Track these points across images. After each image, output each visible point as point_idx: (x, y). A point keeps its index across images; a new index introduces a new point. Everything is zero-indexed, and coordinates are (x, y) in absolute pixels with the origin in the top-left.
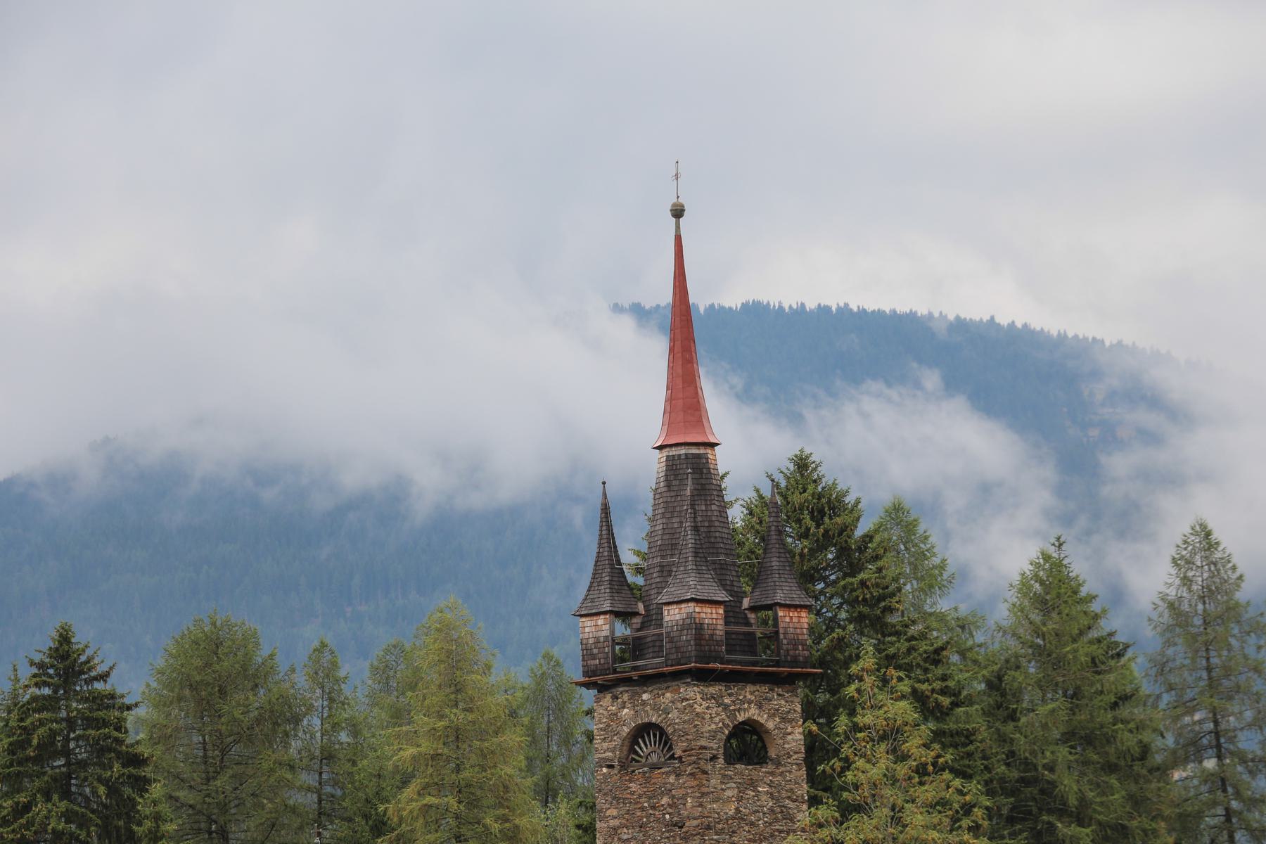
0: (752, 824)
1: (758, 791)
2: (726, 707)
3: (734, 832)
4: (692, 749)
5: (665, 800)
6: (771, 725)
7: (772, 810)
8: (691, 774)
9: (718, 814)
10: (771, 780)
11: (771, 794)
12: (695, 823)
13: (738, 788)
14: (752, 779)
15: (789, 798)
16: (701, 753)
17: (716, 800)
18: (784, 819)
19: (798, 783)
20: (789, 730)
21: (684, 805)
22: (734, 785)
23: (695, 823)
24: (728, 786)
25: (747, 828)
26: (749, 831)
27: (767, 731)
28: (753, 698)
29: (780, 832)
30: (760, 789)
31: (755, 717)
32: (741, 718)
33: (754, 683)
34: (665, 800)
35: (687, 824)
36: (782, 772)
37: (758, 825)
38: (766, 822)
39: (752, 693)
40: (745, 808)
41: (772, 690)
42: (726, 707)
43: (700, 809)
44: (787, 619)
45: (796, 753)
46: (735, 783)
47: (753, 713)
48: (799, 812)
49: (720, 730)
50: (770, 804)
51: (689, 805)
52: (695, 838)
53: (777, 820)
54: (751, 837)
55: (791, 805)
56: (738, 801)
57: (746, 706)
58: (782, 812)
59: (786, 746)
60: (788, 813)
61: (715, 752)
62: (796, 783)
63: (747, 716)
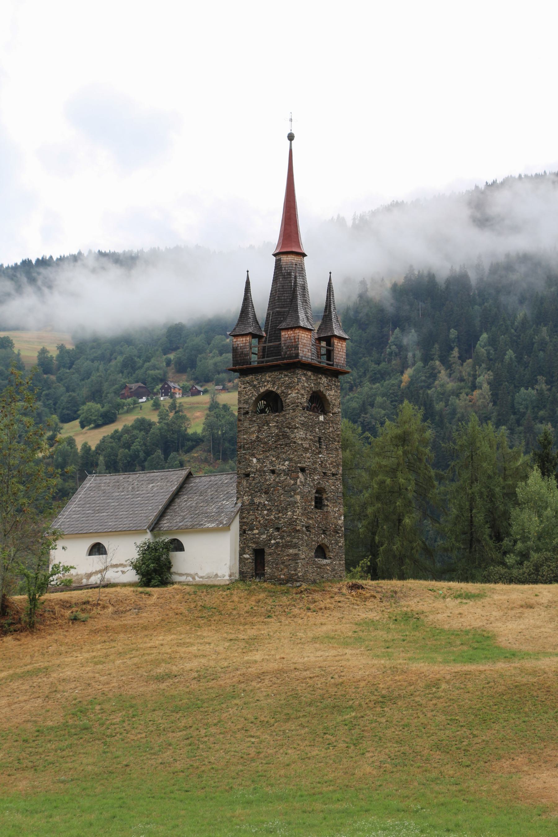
0: (266, 443)
2: (254, 386)
3: (255, 448)
7: (277, 435)
11: (277, 426)
15: (287, 427)
17: (246, 433)
20: (290, 392)
25: (262, 445)
28: (270, 379)
29: (281, 445)
31: (270, 389)
32: (262, 390)
33: (271, 372)
39: (270, 377)
41: (282, 373)
42: (254, 386)
44: (287, 336)
45: (293, 404)
47: (269, 387)
49: (250, 398)
53: (280, 439)
55: (288, 430)
56: (258, 432)
57: (266, 384)
60: (286, 435)
62: (292, 419)
63: (266, 388)
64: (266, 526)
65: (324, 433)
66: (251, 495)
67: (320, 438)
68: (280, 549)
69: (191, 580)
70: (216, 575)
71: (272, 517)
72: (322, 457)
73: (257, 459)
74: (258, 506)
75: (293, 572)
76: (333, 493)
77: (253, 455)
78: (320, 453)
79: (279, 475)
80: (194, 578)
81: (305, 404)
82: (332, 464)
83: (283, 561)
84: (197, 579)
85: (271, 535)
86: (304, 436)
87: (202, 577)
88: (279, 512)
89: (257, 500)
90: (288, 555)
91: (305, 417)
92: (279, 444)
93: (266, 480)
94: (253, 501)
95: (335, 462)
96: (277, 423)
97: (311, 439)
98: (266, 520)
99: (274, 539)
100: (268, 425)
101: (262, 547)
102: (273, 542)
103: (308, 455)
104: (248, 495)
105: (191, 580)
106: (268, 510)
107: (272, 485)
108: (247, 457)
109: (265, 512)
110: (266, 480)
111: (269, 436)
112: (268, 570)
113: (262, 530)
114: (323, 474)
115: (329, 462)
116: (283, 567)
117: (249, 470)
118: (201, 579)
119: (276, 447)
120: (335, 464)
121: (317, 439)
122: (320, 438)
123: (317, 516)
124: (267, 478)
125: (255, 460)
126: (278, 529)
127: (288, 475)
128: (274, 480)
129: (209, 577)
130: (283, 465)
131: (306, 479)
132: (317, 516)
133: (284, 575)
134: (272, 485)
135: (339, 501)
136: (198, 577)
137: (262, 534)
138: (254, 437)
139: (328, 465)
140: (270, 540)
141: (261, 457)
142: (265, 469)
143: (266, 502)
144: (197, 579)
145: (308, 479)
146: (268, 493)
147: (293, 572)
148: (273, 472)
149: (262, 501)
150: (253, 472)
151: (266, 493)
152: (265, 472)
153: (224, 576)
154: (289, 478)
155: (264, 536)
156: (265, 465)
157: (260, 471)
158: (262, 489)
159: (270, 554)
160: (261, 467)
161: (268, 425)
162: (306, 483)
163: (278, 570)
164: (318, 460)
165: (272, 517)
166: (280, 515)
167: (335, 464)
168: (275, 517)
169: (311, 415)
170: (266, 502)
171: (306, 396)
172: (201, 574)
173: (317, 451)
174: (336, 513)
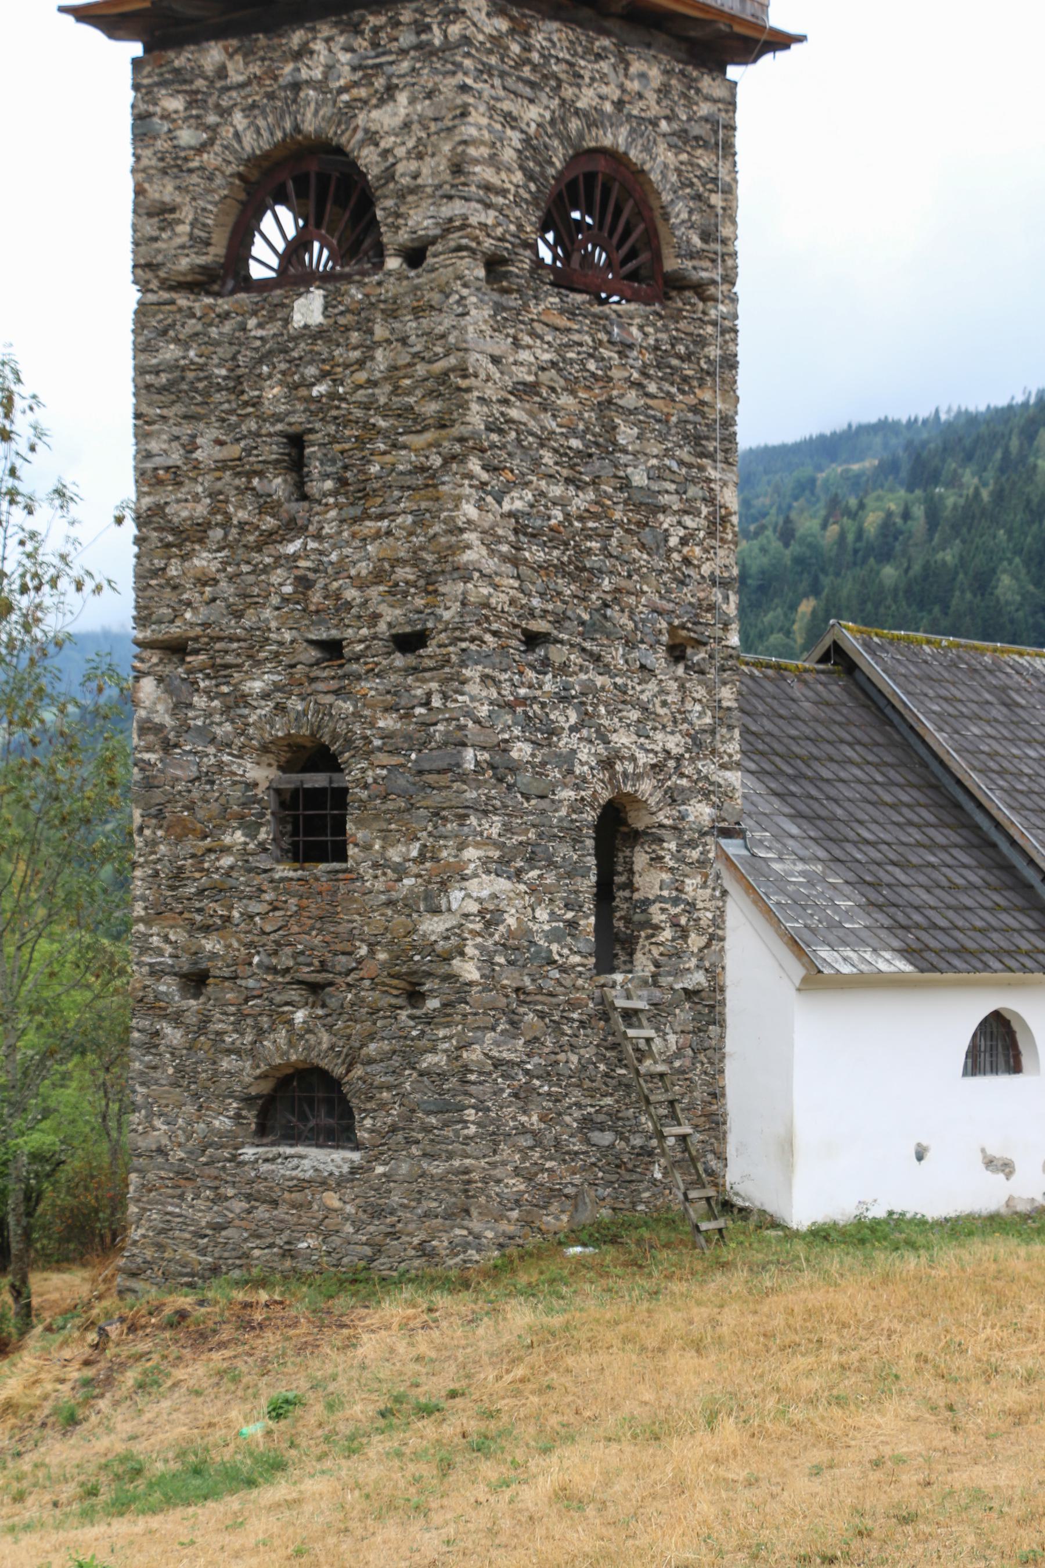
65: (332, 396)
67: (296, 442)
72: (304, 553)
76: (383, 758)
78: (292, 528)
81: (184, 263)
82: (378, 576)
86: (176, 458)
91: (184, 344)
95: (415, 560)
97: (223, 465)
103: (204, 561)
114: (314, 654)
115: (364, 568)
120: (405, 573)
121: (271, 451)
122: (296, 442)
123: (255, 907)
131: (180, 706)
132: (255, 907)
135: (436, 798)
139: (351, 594)
145: (200, 701)
162: (184, 728)
164: (277, 576)
167: (405, 573)
169: (225, 316)
171: (187, 214)
173: (269, 522)
174: (401, 873)
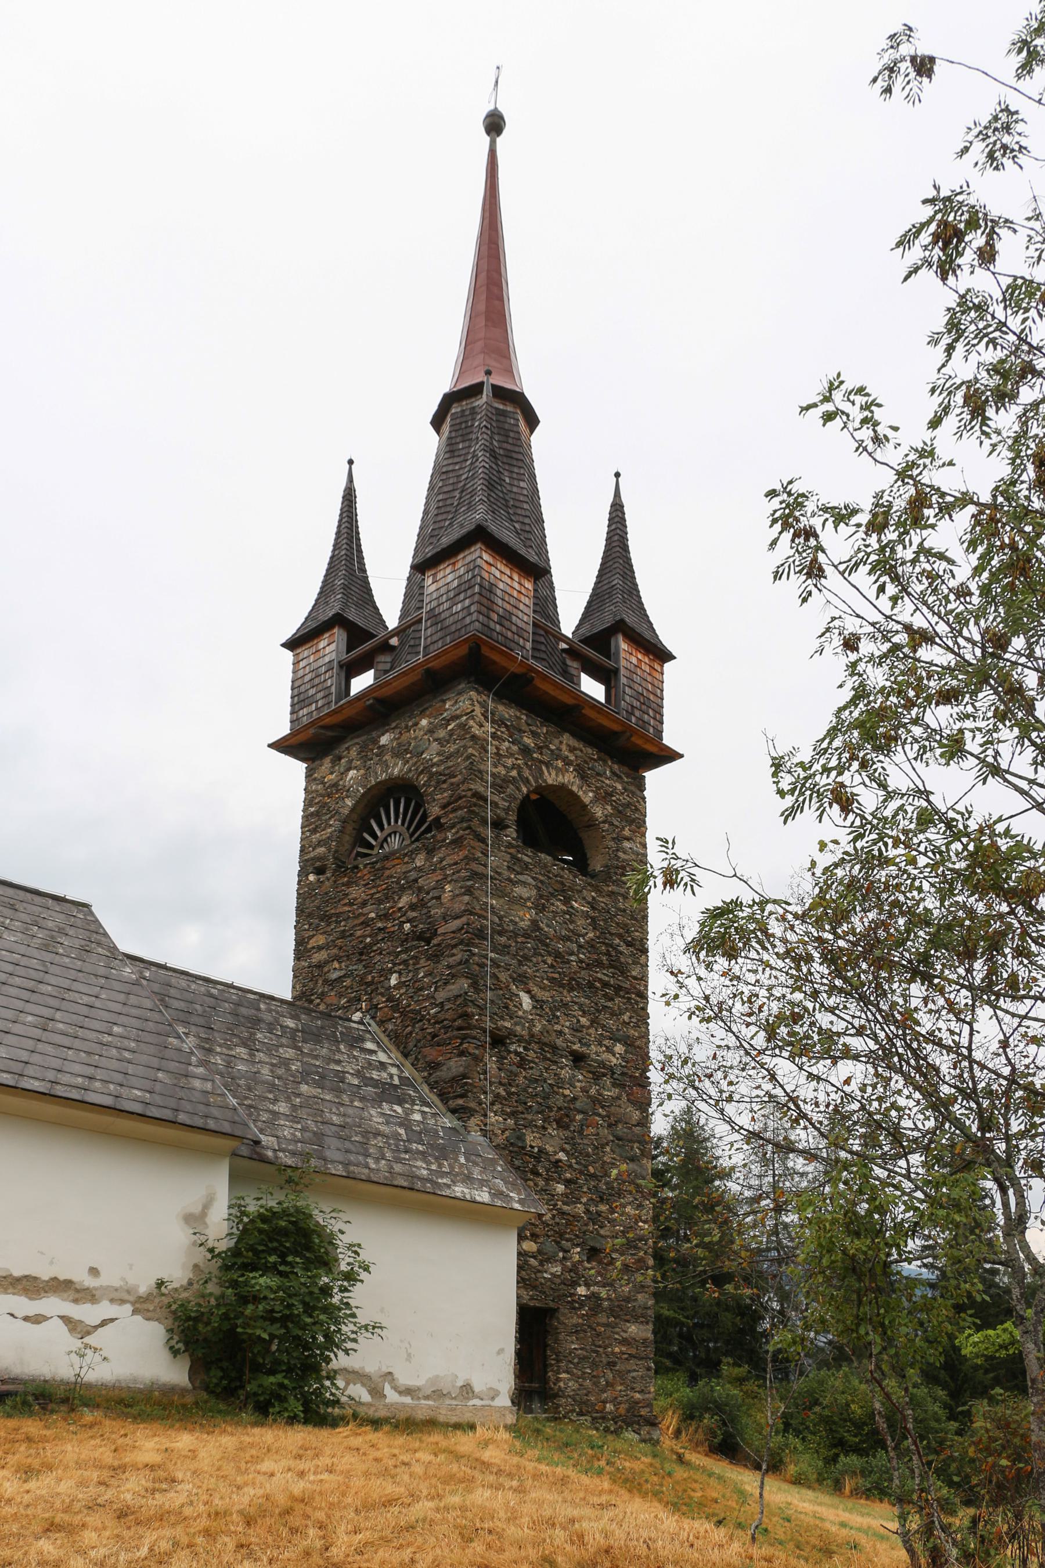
0: (558, 955)
1: (572, 907)
3: (526, 958)
4: (460, 798)
5: (404, 901)
6: (598, 812)
7: (591, 945)
8: (453, 842)
9: (500, 918)
10: (594, 898)
11: (593, 919)
12: (456, 924)
13: (538, 889)
14: (562, 883)
15: (620, 936)
16: (475, 805)
18: (611, 966)
19: (636, 919)
21: (439, 898)
22: (530, 880)
23: (456, 924)
24: (520, 877)
26: (552, 966)
27: (592, 824)
29: (606, 985)
30: (576, 905)
34: (404, 901)
35: (440, 931)
36: (613, 893)
37: (569, 962)
38: (581, 961)
40: (548, 926)
43: (466, 898)
46: (533, 878)
48: (634, 963)
50: (591, 935)
51: (446, 896)
52: (454, 951)
53: (599, 964)
54: (556, 976)
55: (623, 948)
58: (608, 954)
59: (620, 854)
61: (503, 814)
64: (561, 1235)
66: (513, 1114)
68: (602, 1318)
69: (366, 1397)
70: (467, 1390)
71: (580, 1209)
73: (532, 997)
74: (537, 1159)
75: (638, 1396)
77: (521, 979)
79: (597, 1077)
80: (377, 1392)
83: (612, 1359)
84: (391, 1396)
85: (574, 1269)
87: (408, 1391)
88: (602, 1199)
89: (531, 1139)
90: (624, 1342)
92: (600, 980)
93: (560, 1083)
94: (521, 1138)
96: (593, 908)
98: (563, 1213)
99: (587, 1285)
100: (567, 901)
101: (552, 1305)
102: (582, 1290)
104: (503, 1113)
105: (366, 1397)
106: (568, 1182)
107: (578, 1105)
108: (503, 976)
109: (560, 1188)
110: (560, 1083)
111: (568, 939)
112: (565, 1381)
113: (550, 1247)
116: (610, 1376)
117: (508, 1024)
118: (407, 1400)
119: (590, 985)
124: (565, 1073)
125: (526, 1001)
126: (593, 1253)
127: (622, 1086)
128: (584, 1090)
129: (438, 1394)
130: (610, 1050)
133: (614, 1401)
134: (578, 1105)
136: (395, 1388)
137: (548, 1260)
138: (525, 917)
140: (575, 1284)
141: (544, 995)
142: (559, 1042)
143: (562, 1156)
144: (391, 1396)
146: (566, 1127)
147: (638, 1396)
148: (578, 1059)
149: (550, 1149)
150: (520, 1040)
151: (561, 1125)
152: (554, 1048)
153: (494, 1394)
154: (624, 1097)
155: (557, 1269)
156: (557, 1027)
157: (542, 1044)
158: (550, 1108)
159: (577, 1331)
160: (545, 1031)
161: (567, 901)
163: (596, 1384)
165: (580, 1209)
166: (603, 1208)
168: (587, 1211)
170: (562, 1156)
172: (405, 1379)
